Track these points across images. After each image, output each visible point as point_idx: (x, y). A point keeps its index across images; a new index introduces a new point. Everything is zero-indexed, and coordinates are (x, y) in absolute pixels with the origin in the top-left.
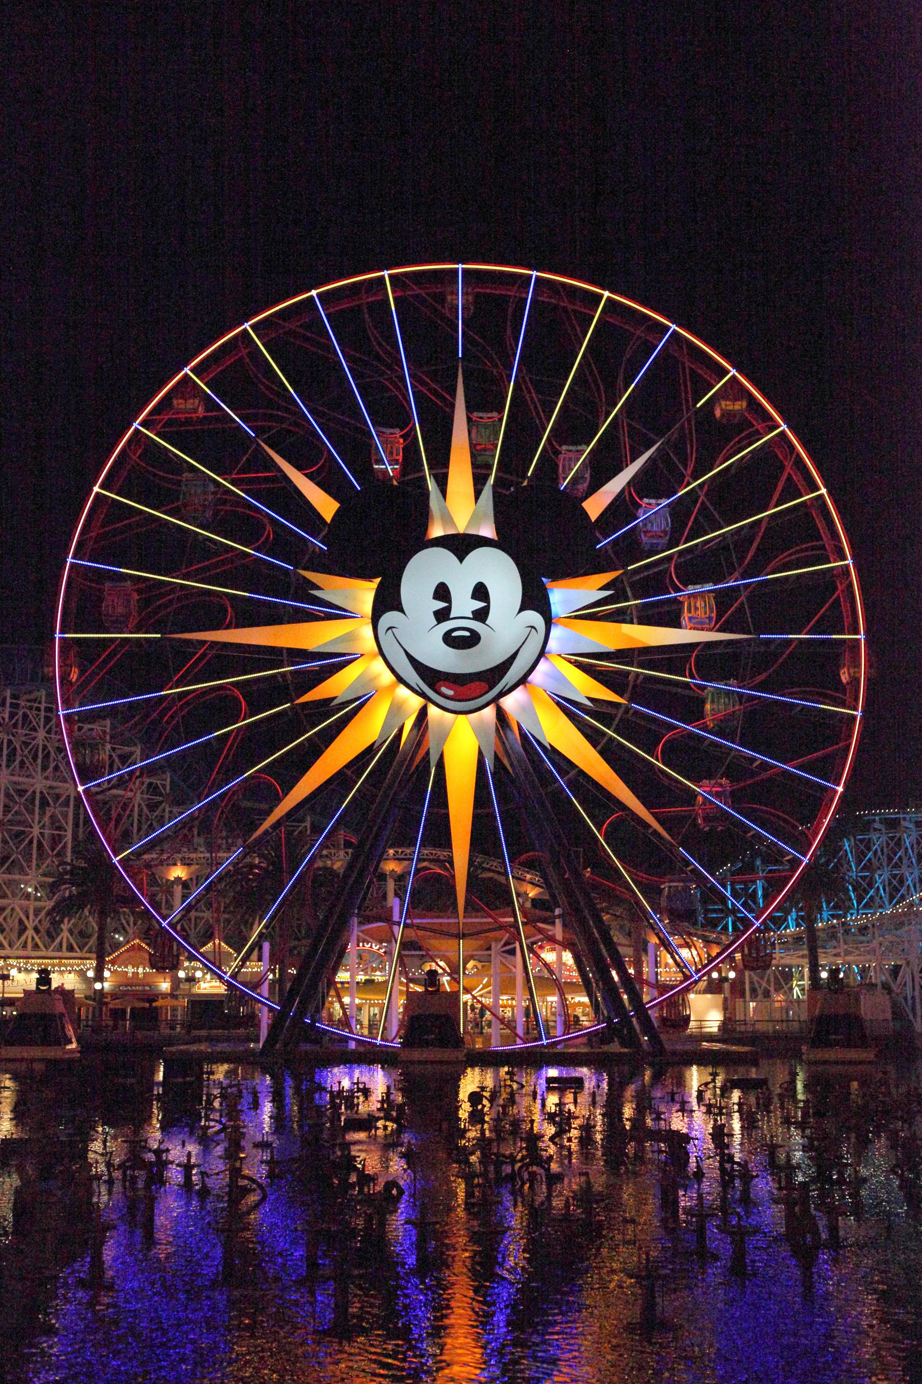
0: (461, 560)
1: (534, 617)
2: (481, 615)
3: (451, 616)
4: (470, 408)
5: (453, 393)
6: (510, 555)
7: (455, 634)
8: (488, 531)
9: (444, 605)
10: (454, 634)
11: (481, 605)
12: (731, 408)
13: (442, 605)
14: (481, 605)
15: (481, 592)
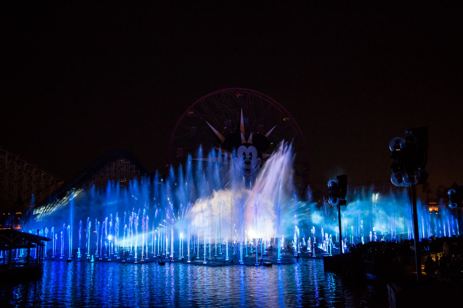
0: (247, 148)
1: (260, 159)
2: (251, 158)
3: (246, 158)
4: (243, 117)
5: (241, 115)
6: (255, 147)
7: (247, 162)
8: (251, 143)
9: (245, 156)
10: (247, 162)
11: (250, 156)
12: (287, 119)
13: (245, 156)
14: (250, 156)
15: (251, 154)
